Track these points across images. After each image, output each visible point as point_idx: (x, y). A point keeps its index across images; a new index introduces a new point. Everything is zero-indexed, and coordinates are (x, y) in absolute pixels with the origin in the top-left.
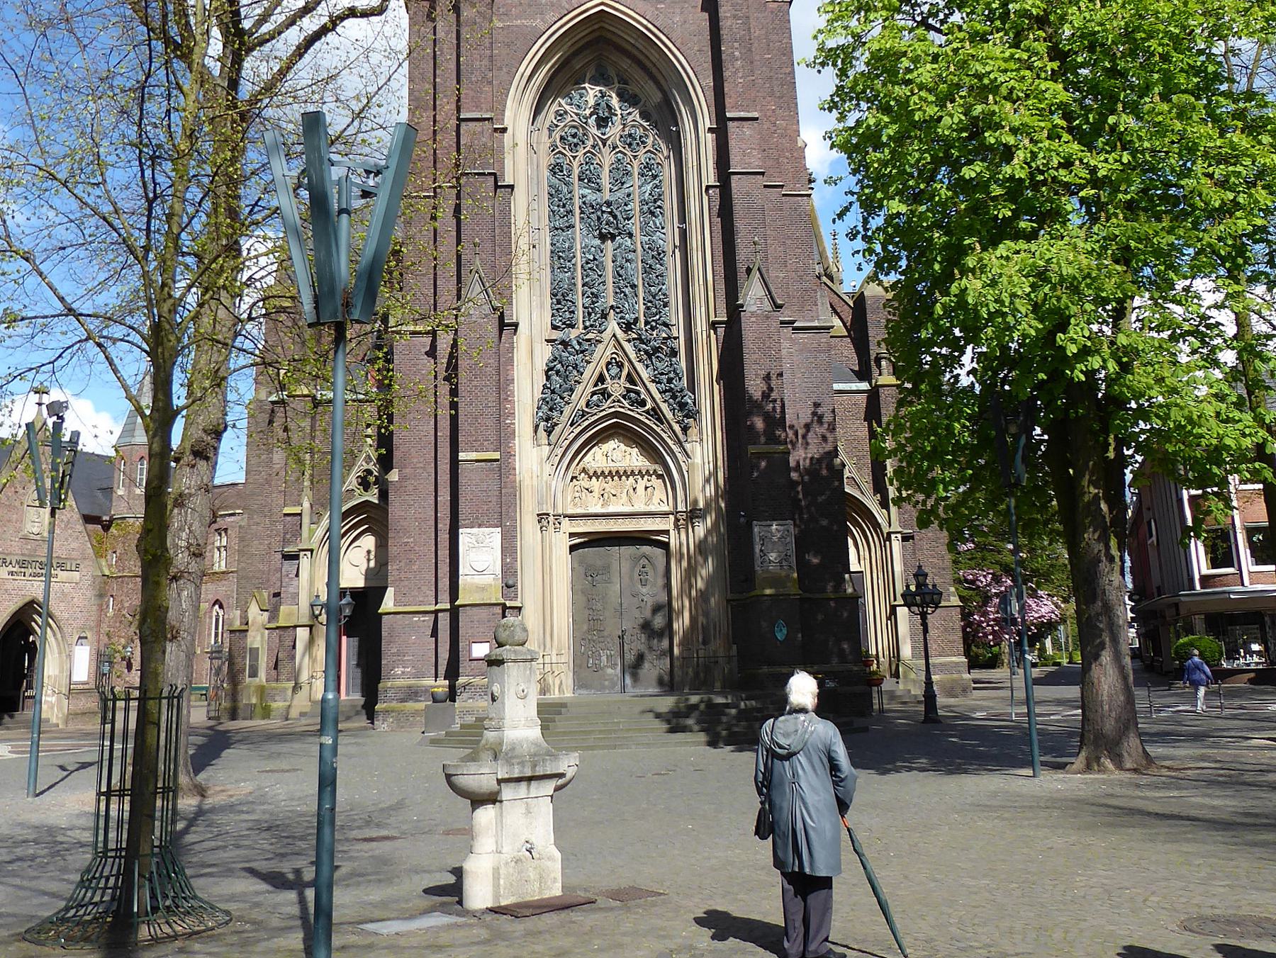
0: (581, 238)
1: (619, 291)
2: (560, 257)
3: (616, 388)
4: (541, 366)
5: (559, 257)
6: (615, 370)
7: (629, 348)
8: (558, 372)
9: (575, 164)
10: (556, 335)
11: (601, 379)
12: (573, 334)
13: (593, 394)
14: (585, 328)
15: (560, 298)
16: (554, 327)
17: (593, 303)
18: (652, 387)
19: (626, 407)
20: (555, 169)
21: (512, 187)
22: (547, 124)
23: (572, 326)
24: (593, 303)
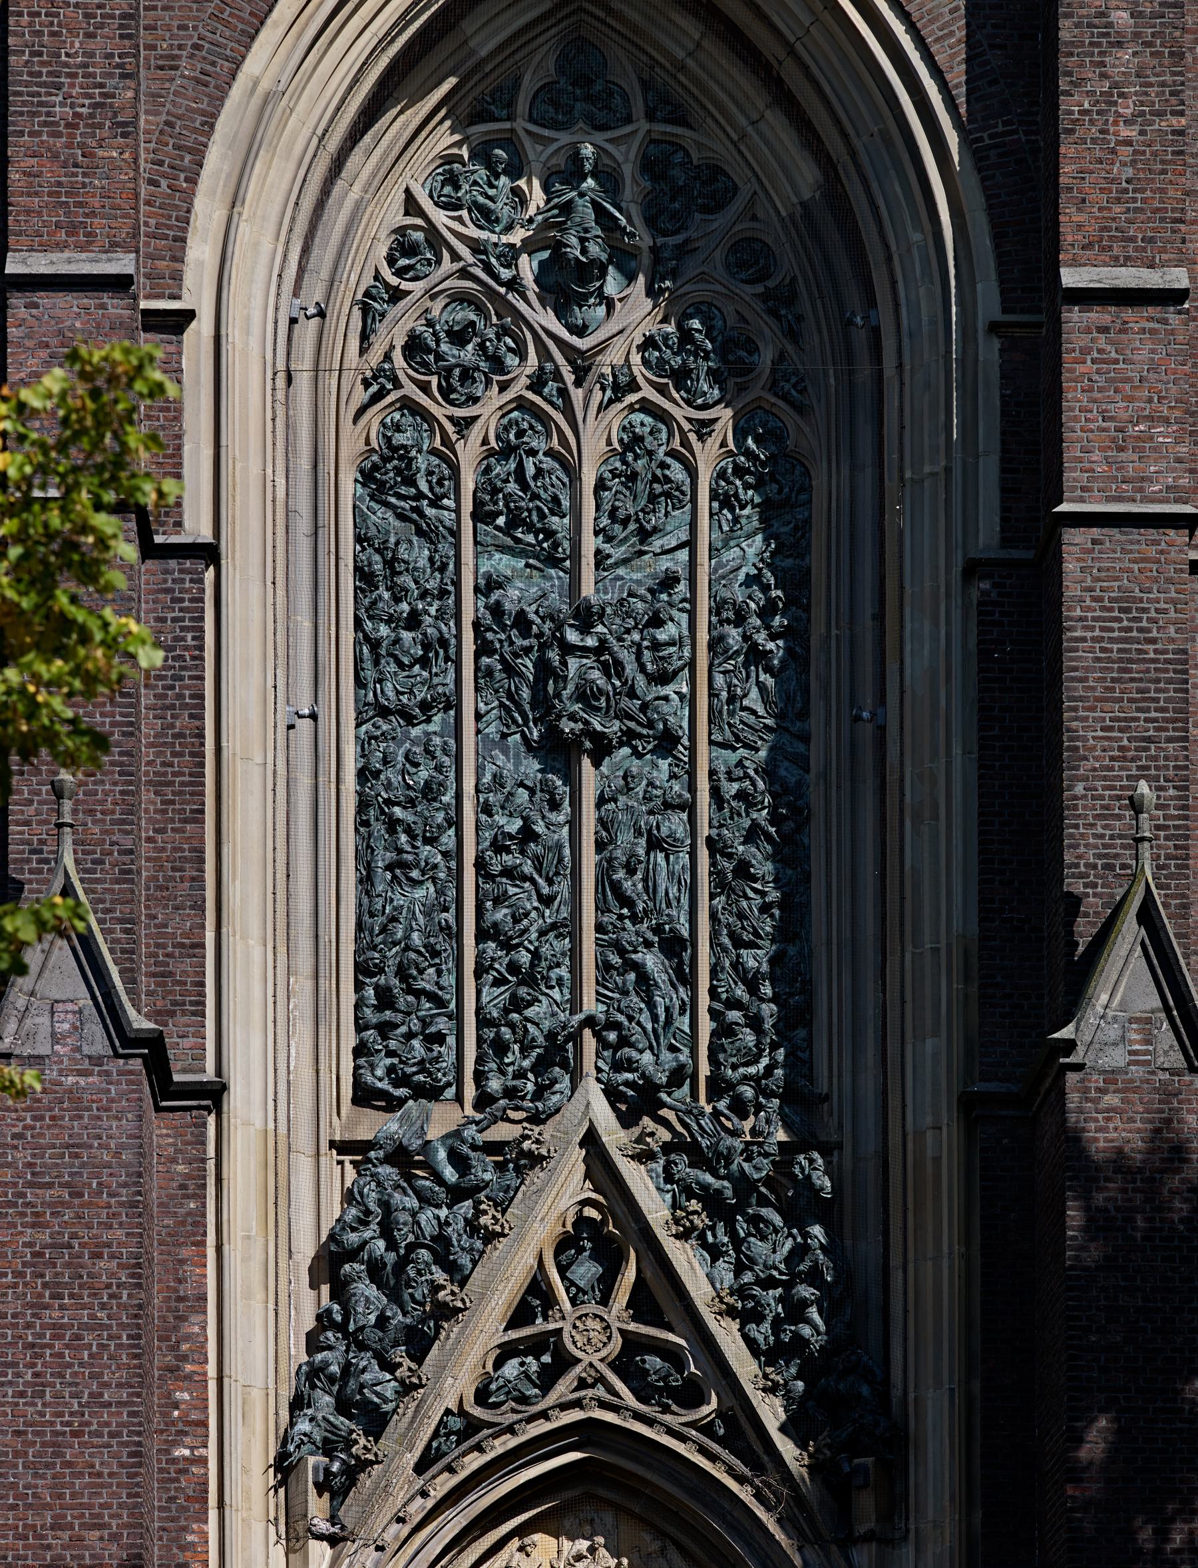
0: (482, 754)
1: (619, 963)
2: (393, 822)
3: (593, 1333)
4: (306, 1250)
5: (392, 825)
6: (586, 1271)
7: (641, 1182)
8: (375, 1271)
9: (469, 454)
10: (372, 1125)
11: (536, 1299)
12: (442, 1120)
13: (506, 1352)
14: (484, 1100)
15: (390, 988)
16: (364, 1096)
17: (517, 1004)
18: (728, 1337)
19: (624, 1408)
20: (385, 474)
21: (210, 553)
22: (356, 280)
23: (432, 1093)
24: (517, 1004)
